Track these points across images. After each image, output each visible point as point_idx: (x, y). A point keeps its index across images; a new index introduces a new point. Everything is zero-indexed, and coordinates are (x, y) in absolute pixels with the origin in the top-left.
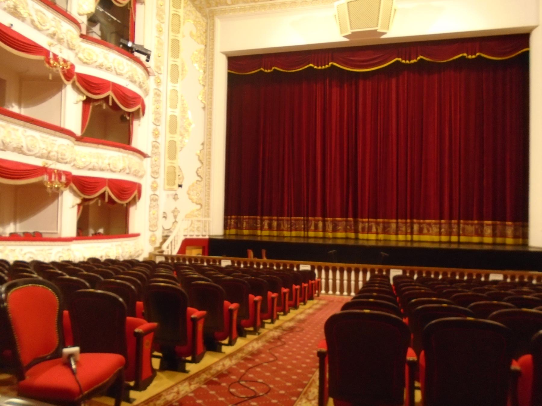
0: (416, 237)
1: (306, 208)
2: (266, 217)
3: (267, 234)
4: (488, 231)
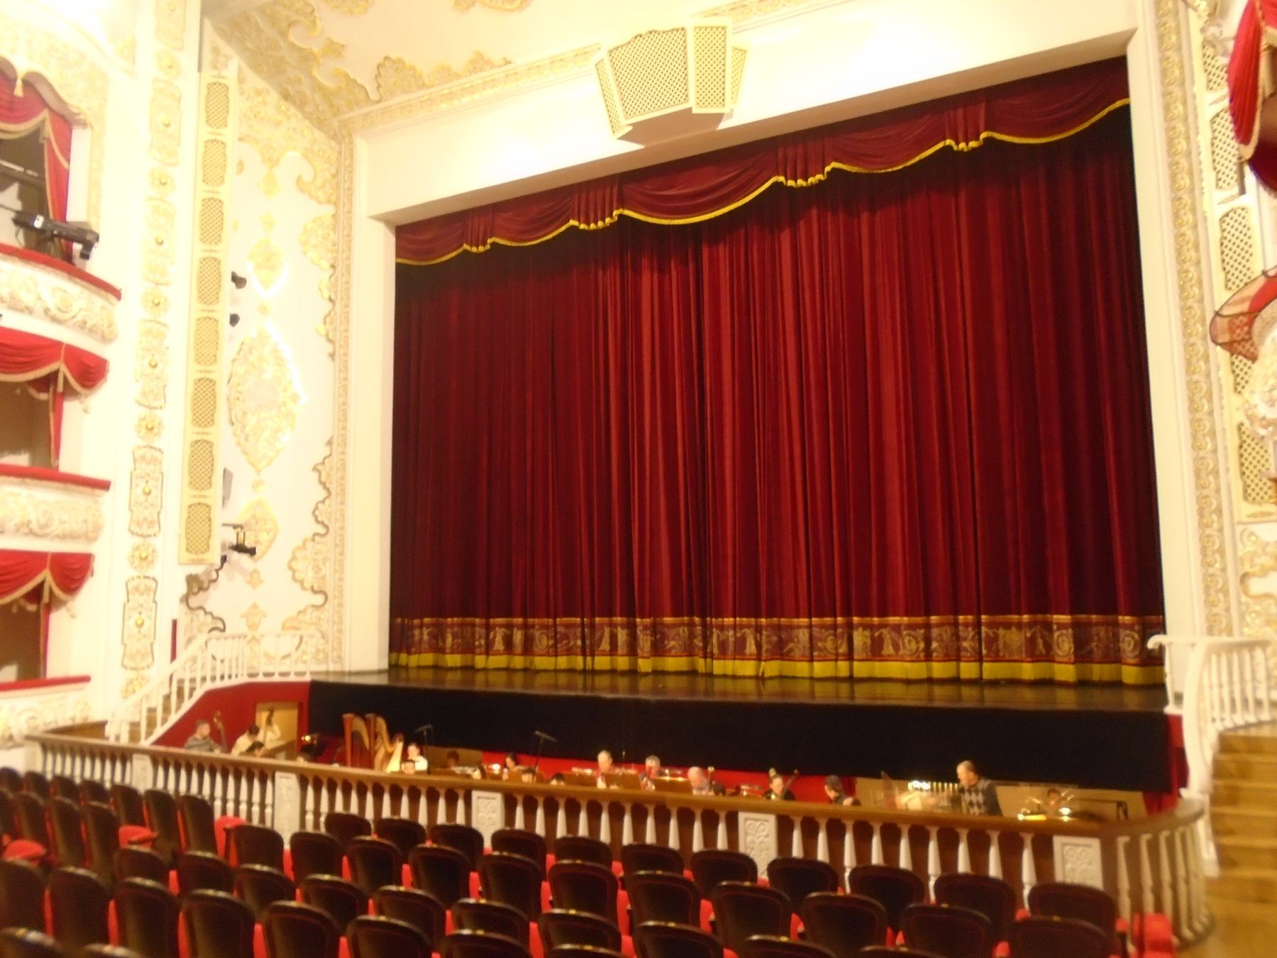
0: (861, 669)
2: (500, 620)
3: (504, 665)
4: (1064, 644)
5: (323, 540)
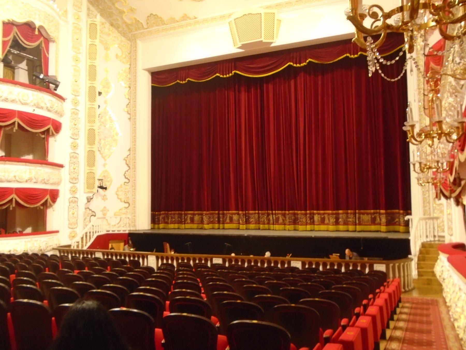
1: (219, 204)
5: (128, 184)
